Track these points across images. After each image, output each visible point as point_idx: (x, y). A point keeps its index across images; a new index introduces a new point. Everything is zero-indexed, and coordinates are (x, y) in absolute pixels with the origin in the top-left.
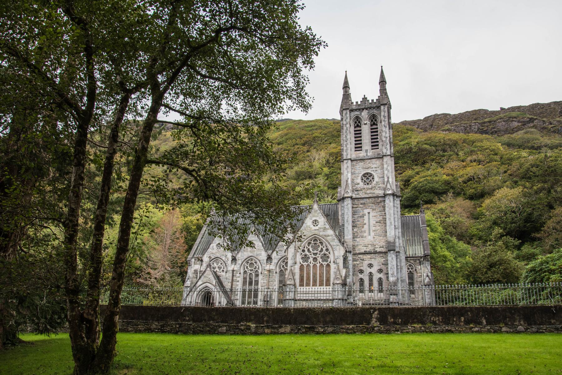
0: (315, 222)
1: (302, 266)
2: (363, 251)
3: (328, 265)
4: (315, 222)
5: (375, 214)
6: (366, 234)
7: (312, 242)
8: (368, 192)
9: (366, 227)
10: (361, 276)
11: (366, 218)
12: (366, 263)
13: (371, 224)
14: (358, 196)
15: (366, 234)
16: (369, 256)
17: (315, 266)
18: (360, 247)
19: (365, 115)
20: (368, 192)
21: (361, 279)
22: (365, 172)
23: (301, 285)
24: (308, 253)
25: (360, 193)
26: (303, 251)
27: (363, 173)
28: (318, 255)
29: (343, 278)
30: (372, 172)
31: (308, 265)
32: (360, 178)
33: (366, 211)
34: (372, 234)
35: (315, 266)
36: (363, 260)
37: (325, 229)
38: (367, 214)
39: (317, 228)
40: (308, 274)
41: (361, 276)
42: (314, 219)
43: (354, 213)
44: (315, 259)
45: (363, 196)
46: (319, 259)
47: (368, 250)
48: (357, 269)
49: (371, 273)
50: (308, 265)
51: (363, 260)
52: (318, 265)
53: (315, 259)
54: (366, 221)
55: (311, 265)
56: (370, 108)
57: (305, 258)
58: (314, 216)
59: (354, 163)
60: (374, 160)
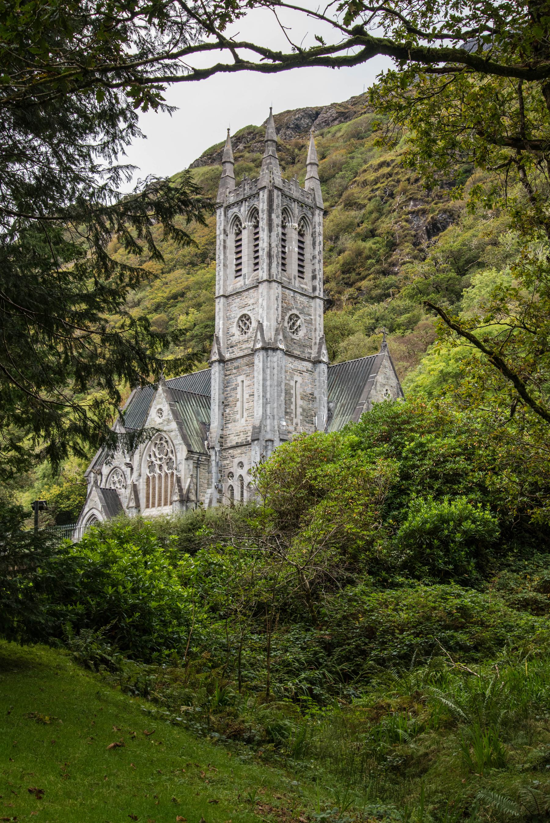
0: (160, 411)
1: (148, 478)
2: (234, 443)
3: (172, 474)
4: (160, 411)
5: (249, 382)
6: (238, 416)
7: (158, 442)
8: (244, 346)
9: (239, 404)
10: (230, 482)
11: (239, 389)
12: (236, 461)
13: (245, 401)
14: (233, 356)
15: (238, 416)
16: (239, 451)
17: (160, 476)
18: (232, 437)
19: (243, 211)
20: (244, 346)
21: (231, 486)
22: (241, 314)
23: (148, 507)
24: (153, 459)
25: (235, 349)
26: (150, 456)
27: (239, 316)
28: (164, 461)
29: (185, 492)
30: (249, 313)
31: (154, 477)
32: (235, 324)
33: (240, 379)
34: (245, 414)
35: (160, 476)
36: (233, 457)
37: (169, 421)
38: (240, 384)
39: (160, 421)
40: (154, 488)
41: (230, 482)
42: (158, 407)
43: (225, 385)
44: (160, 467)
45: (238, 355)
46: (165, 467)
47: (240, 441)
48: (227, 471)
49: (241, 476)
50: (154, 477)
51: (233, 457)
52: (163, 475)
53: (160, 467)
54: (239, 396)
55: (156, 475)
56: (249, 197)
57: (151, 466)
58: (159, 403)
59: (230, 300)
60: (252, 291)
